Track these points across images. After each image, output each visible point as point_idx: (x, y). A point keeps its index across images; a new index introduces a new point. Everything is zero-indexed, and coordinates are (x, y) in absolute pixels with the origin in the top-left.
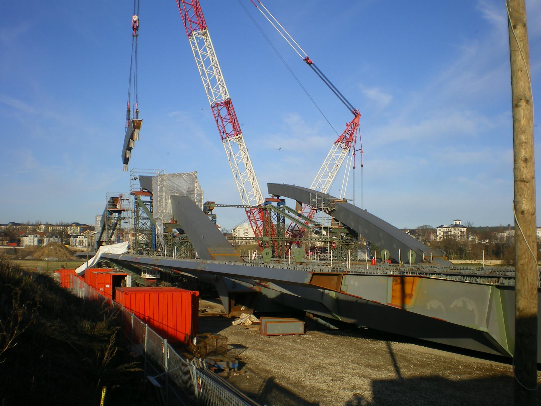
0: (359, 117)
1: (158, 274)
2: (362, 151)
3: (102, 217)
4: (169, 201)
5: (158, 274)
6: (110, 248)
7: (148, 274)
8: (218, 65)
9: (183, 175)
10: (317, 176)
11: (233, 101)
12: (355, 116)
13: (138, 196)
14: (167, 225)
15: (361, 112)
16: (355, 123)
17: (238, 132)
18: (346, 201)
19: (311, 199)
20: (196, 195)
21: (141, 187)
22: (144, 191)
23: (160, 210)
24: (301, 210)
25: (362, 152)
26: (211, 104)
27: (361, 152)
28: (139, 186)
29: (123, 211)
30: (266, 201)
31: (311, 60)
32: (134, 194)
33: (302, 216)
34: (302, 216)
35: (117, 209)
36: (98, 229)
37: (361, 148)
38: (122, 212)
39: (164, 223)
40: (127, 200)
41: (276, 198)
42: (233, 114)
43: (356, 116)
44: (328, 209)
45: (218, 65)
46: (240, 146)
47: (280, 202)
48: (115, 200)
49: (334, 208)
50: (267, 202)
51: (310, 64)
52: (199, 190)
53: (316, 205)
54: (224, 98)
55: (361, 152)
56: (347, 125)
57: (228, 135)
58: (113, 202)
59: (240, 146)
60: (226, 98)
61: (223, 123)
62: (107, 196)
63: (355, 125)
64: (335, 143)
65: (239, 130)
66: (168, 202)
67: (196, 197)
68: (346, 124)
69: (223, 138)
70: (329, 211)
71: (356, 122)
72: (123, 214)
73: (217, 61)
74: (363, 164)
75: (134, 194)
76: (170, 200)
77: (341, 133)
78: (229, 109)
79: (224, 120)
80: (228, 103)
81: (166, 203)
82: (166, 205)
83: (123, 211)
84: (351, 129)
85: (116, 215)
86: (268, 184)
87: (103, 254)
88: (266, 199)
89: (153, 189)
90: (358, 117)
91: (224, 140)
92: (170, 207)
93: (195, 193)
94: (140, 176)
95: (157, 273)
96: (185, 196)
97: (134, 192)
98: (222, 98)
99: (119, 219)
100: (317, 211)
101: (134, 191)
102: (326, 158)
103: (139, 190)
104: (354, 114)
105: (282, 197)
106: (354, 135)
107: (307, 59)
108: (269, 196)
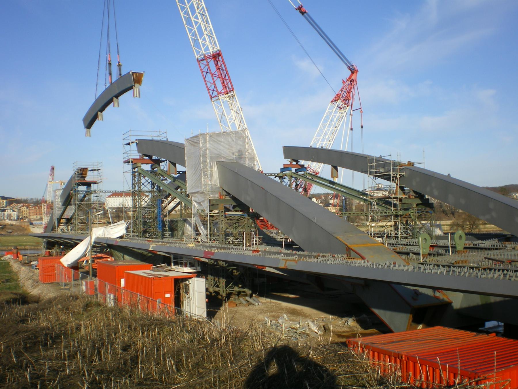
0: (356, 73)
1: (199, 266)
2: (361, 110)
3: (62, 191)
4: (215, 169)
5: (199, 266)
6: (105, 230)
7: (186, 267)
8: (206, 12)
9: (231, 134)
10: (314, 138)
11: (223, 54)
12: (350, 72)
13: (139, 165)
14: (215, 201)
15: (358, 68)
16: (353, 79)
17: (228, 89)
18: (414, 165)
19: (369, 163)
20: (247, 160)
21: (139, 152)
22: (144, 158)
23: (205, 181)
24: (337, 176)
25: (361, 112)
26: (197, 57)
27: (360, 112)
28: (137, 152)
29: (92, 183)
30: (284, 168)
31: (304, 9)
32: (132, 162)
33: (335, 184)
34: (335, 184)
35: (86, 181)
36: (58, 204)
37: (360, 108)
38: (92, 185)
39: (210, 198)
40: (98, 170)
41: (294, 163)
42: (224, 69)
43: (353, 73)
44: (397, 174)
45: (206, 12)
46: (231, 106)
47: (299, 168)
48: (83, 171)
49: (403, 174)
50: (286, 168)
51: (303, 13)
52: (251, 153)
53: (375, 170)
54: (211, 51)
55: (360, 112)
56: (344, 82)
57: (219, 93)
58: (82, 174)
59: (231, 106)
60: (215, 50)
61: (213, 79)
62: (73, 167)
63: (352, 81)
65: (230, 87)
66: (214, 170)
67: (248, 163)
68: (342, 81)
69: (212, 96)
70: (399, 177)
71: (354, 79)
72: (94, 187)
73: (205, 7)
74: (363, 125)
75: (132, 162)
76: (216, 168)
77: (338, 91)
78: (217, 63)
79: (213, 75)
80: (216, 56)
81: (211, 171)
82: (211, 175)
83: (92, 183)
84: (348, 87)
85: (83, 188)
86: (283, 147)
87: (97, 238)
88: (284, 164)
89: (185, 153)
90: (355, 73)
91: (212, 99)
92: (217, 177)
93: (246, 158)
94: (136, 140)
95: (196, 264)
96: (235, 161)
97: (132, 160)
98: (209, 50)
99: (88, 193)
100: (376, 178)
101: (132, 159)
102: (323, 118)
103: (138, 157)
104: (350, 69)
105: (302, 162)
106: (351, 94)
107: (300, 8)
108: (287, 162)
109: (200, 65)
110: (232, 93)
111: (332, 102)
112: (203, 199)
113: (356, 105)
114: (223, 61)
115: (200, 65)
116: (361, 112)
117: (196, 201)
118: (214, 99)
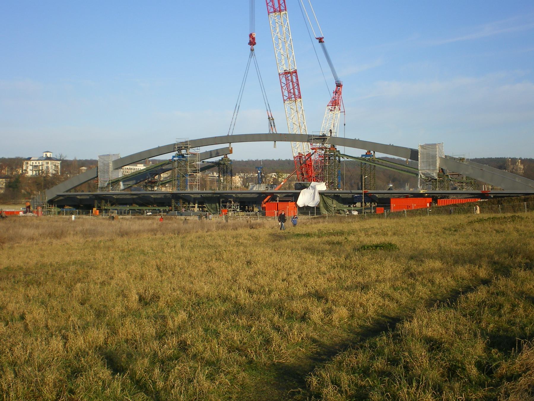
25: (345, 114)
31: (323, 40)
64: (328, 106)
89: (419, 151)
104: (336, 84)
109: (280, 78)
110: (299, 100)
111: (328, 106)
112: (431, 173)
113: (342, 110)
114: (297, 77)
115: (280, 78)
116: (345, 114)
117: (422, 173)
118: (286, 102)
